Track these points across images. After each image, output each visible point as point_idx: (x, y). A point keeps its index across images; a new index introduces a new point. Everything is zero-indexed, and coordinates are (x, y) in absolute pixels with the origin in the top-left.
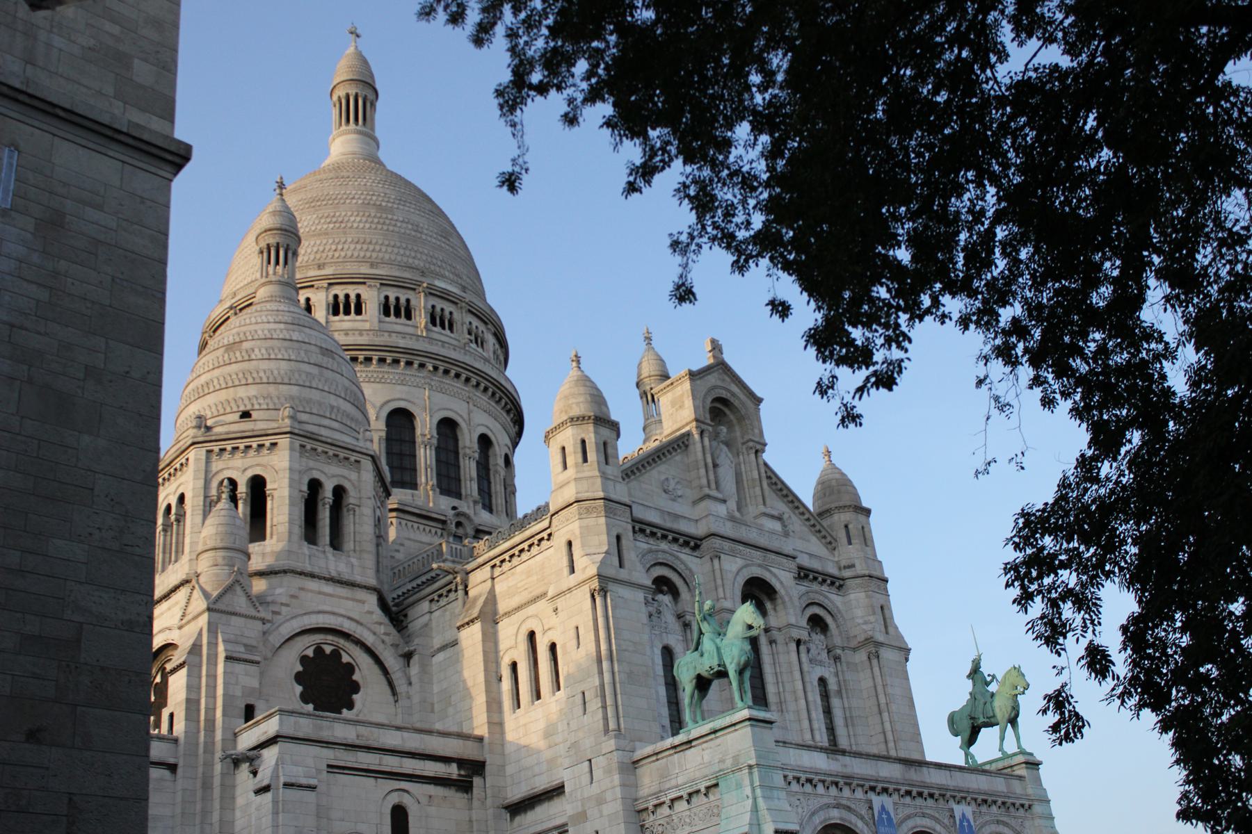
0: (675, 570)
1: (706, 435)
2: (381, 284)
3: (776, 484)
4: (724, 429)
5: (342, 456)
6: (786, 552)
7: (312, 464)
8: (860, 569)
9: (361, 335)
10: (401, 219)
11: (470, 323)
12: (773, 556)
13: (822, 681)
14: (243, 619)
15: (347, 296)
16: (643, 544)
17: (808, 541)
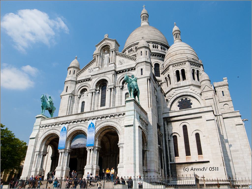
0: (86, 86)
6: (111, 70)
12: (107, 73)
17: (129, 62)
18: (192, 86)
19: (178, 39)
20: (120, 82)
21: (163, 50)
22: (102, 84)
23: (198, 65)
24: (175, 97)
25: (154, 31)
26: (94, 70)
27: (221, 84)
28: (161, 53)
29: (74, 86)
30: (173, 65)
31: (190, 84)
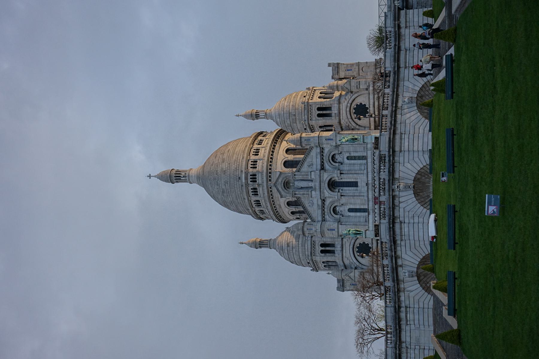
0: (330, 207)
1: (295, 193)
2: (249, 196)
3: (300, 167)
4: (291, 184)
5: (313, 246)
6: (319, 174)
7: (317, 253)
8: (317, 145)
9: (267, 204)
10: (225, 187)
11: (251, 168)
12: (321, 179)
13: (348, 158)
14: (355, 274)
15: (255, 203)
16: (327, 217)
17: (312, 156)
18: (341, 101)
19: (266, 113)
20: (333, 165)
21: (263, 143)
22: (333, 185)
23: (314, 92)
24: (350, 120)
25: (223, 154)
26: (313, 196)
27: (336, 71)
28: (269, 145)
29: (329, 222)
30: (309, 120)
31: (337, 102)
